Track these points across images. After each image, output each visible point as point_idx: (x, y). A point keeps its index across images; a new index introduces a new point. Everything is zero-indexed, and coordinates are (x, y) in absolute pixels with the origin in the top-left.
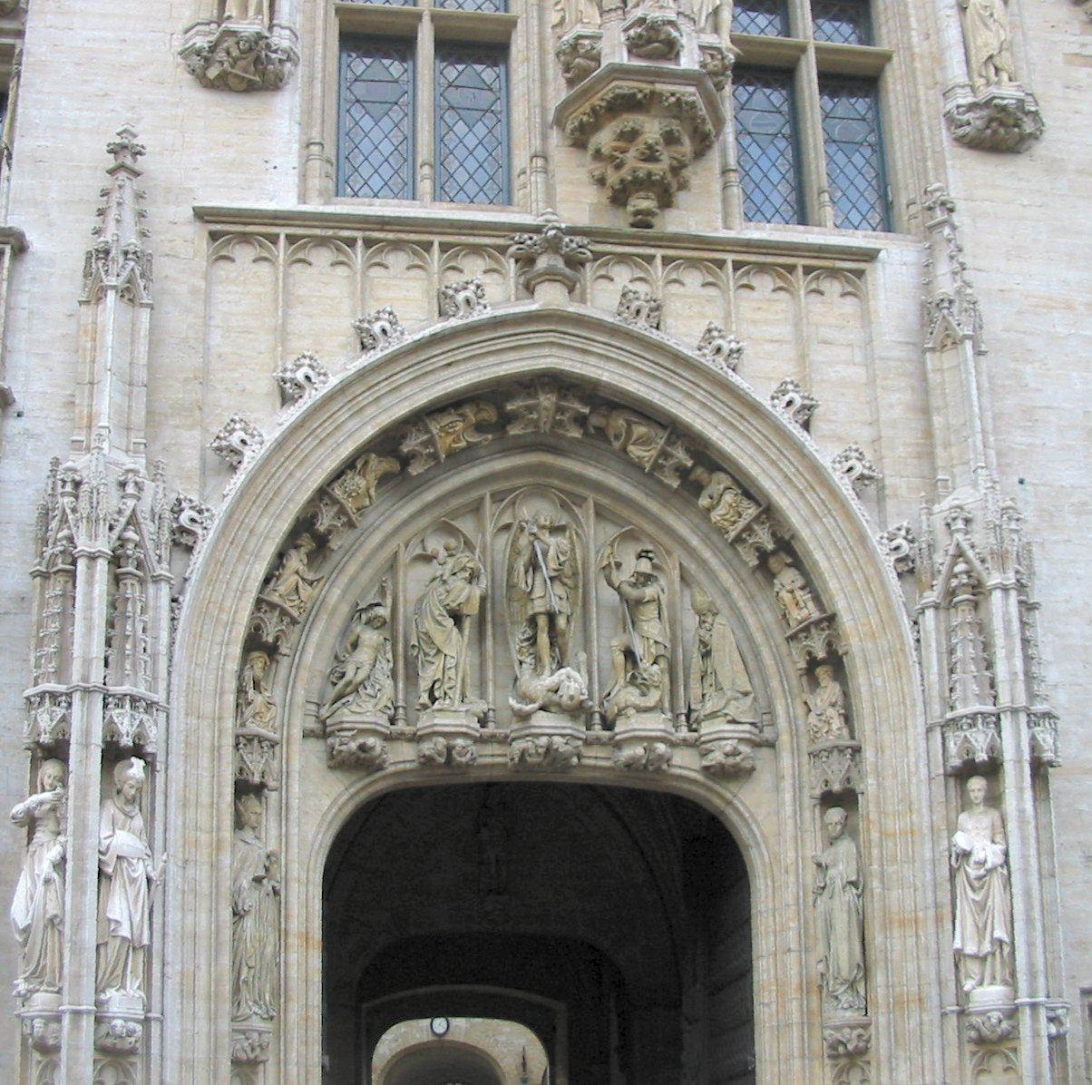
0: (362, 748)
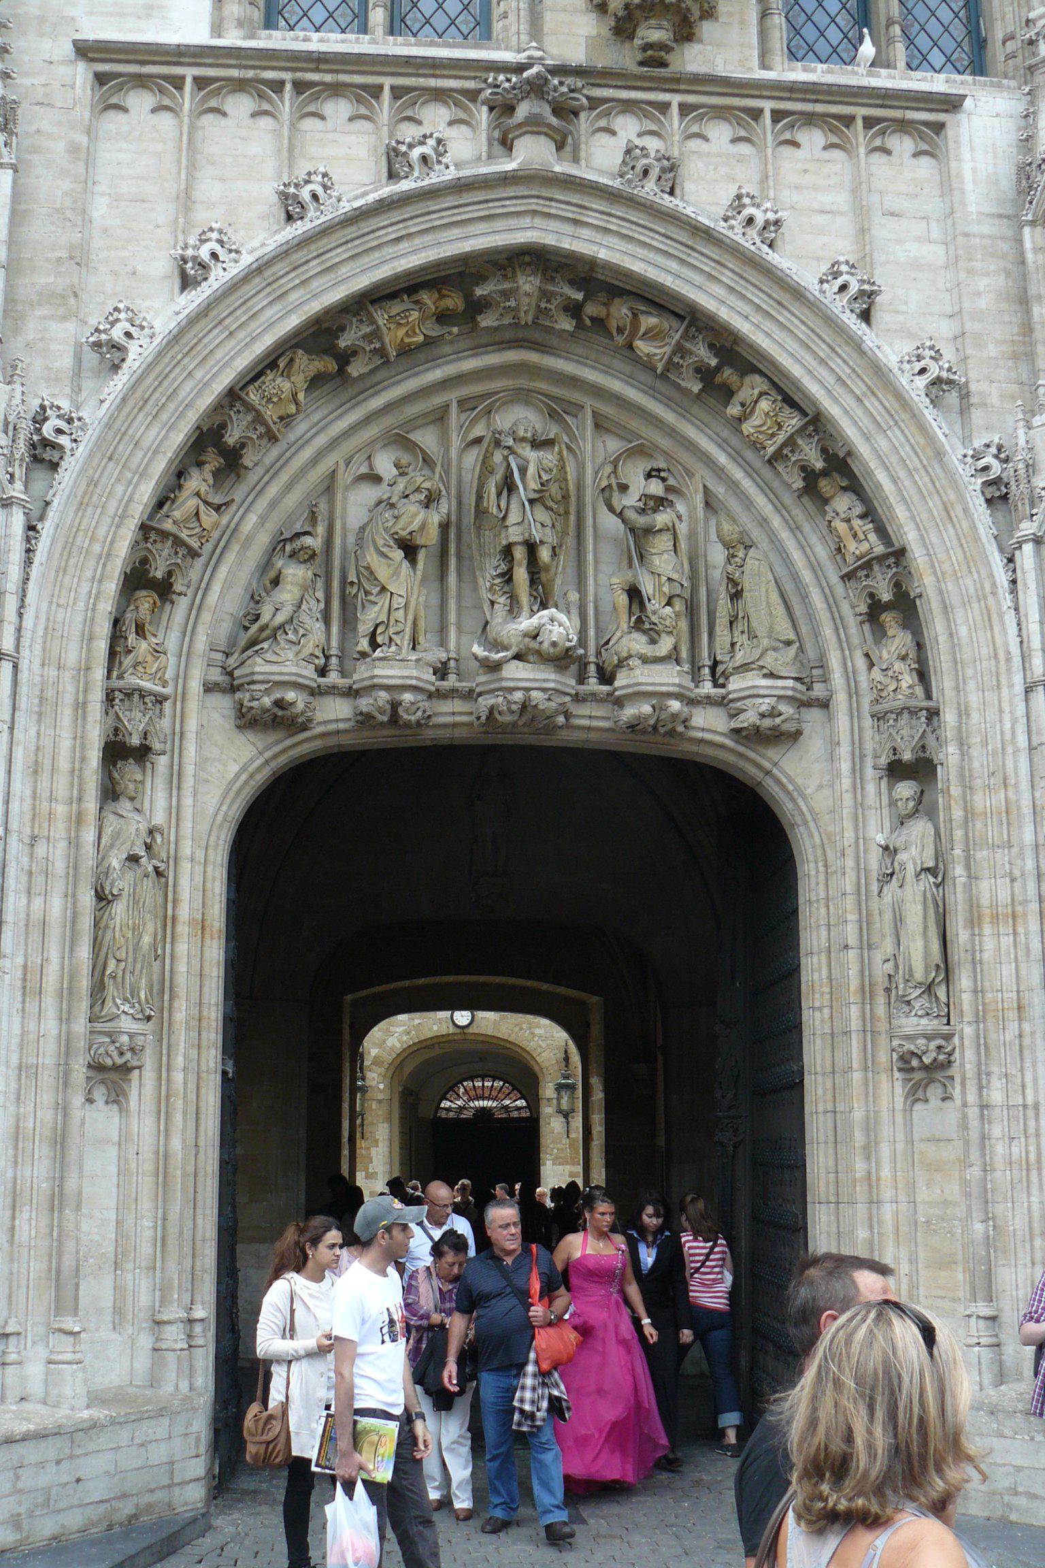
0: (279, 704)
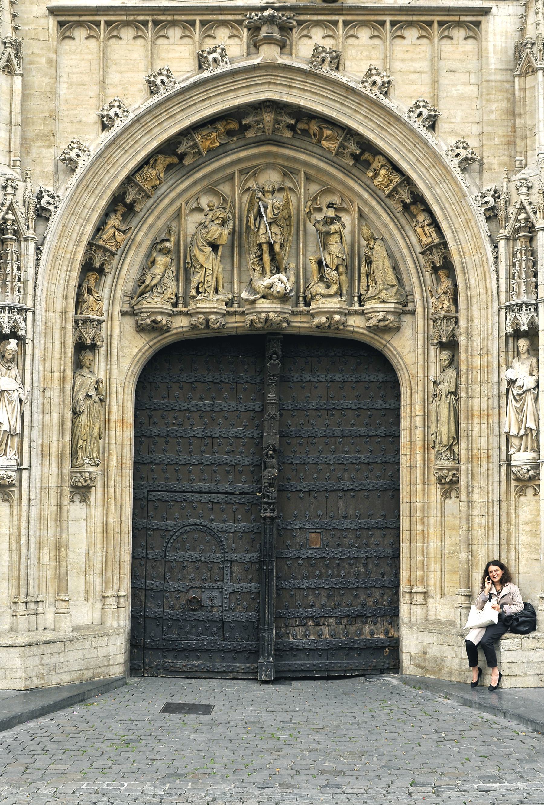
0: (154, 321)
